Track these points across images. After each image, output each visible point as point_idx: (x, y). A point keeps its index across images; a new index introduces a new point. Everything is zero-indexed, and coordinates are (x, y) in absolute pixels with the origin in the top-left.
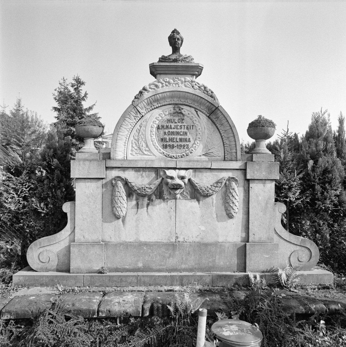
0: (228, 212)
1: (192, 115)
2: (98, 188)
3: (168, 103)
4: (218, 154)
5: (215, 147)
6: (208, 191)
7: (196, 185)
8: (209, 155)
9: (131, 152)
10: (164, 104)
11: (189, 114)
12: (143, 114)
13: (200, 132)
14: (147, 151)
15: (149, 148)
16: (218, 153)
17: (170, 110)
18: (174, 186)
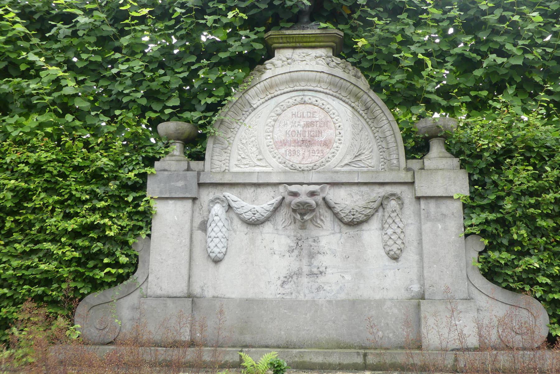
0: (388, 249)
1: (328, 106)
2: (185, 212)
3: (291, 89)
4: (370, 163)
5: (364, 152)
6: (353, 215)
7: (336, 206)
8: (355, 164)
9: (237, 163)
10: (286, 90)
11: (323, 105)
12: (255, 106)
13: (341, 131)
14: (261, 159)
15: (263, 156)
16: (369, 160)
17: (296, 100)
18: (298, 206)
